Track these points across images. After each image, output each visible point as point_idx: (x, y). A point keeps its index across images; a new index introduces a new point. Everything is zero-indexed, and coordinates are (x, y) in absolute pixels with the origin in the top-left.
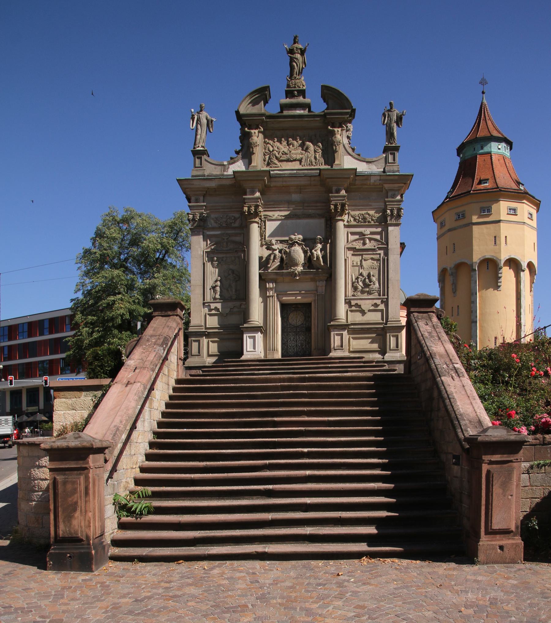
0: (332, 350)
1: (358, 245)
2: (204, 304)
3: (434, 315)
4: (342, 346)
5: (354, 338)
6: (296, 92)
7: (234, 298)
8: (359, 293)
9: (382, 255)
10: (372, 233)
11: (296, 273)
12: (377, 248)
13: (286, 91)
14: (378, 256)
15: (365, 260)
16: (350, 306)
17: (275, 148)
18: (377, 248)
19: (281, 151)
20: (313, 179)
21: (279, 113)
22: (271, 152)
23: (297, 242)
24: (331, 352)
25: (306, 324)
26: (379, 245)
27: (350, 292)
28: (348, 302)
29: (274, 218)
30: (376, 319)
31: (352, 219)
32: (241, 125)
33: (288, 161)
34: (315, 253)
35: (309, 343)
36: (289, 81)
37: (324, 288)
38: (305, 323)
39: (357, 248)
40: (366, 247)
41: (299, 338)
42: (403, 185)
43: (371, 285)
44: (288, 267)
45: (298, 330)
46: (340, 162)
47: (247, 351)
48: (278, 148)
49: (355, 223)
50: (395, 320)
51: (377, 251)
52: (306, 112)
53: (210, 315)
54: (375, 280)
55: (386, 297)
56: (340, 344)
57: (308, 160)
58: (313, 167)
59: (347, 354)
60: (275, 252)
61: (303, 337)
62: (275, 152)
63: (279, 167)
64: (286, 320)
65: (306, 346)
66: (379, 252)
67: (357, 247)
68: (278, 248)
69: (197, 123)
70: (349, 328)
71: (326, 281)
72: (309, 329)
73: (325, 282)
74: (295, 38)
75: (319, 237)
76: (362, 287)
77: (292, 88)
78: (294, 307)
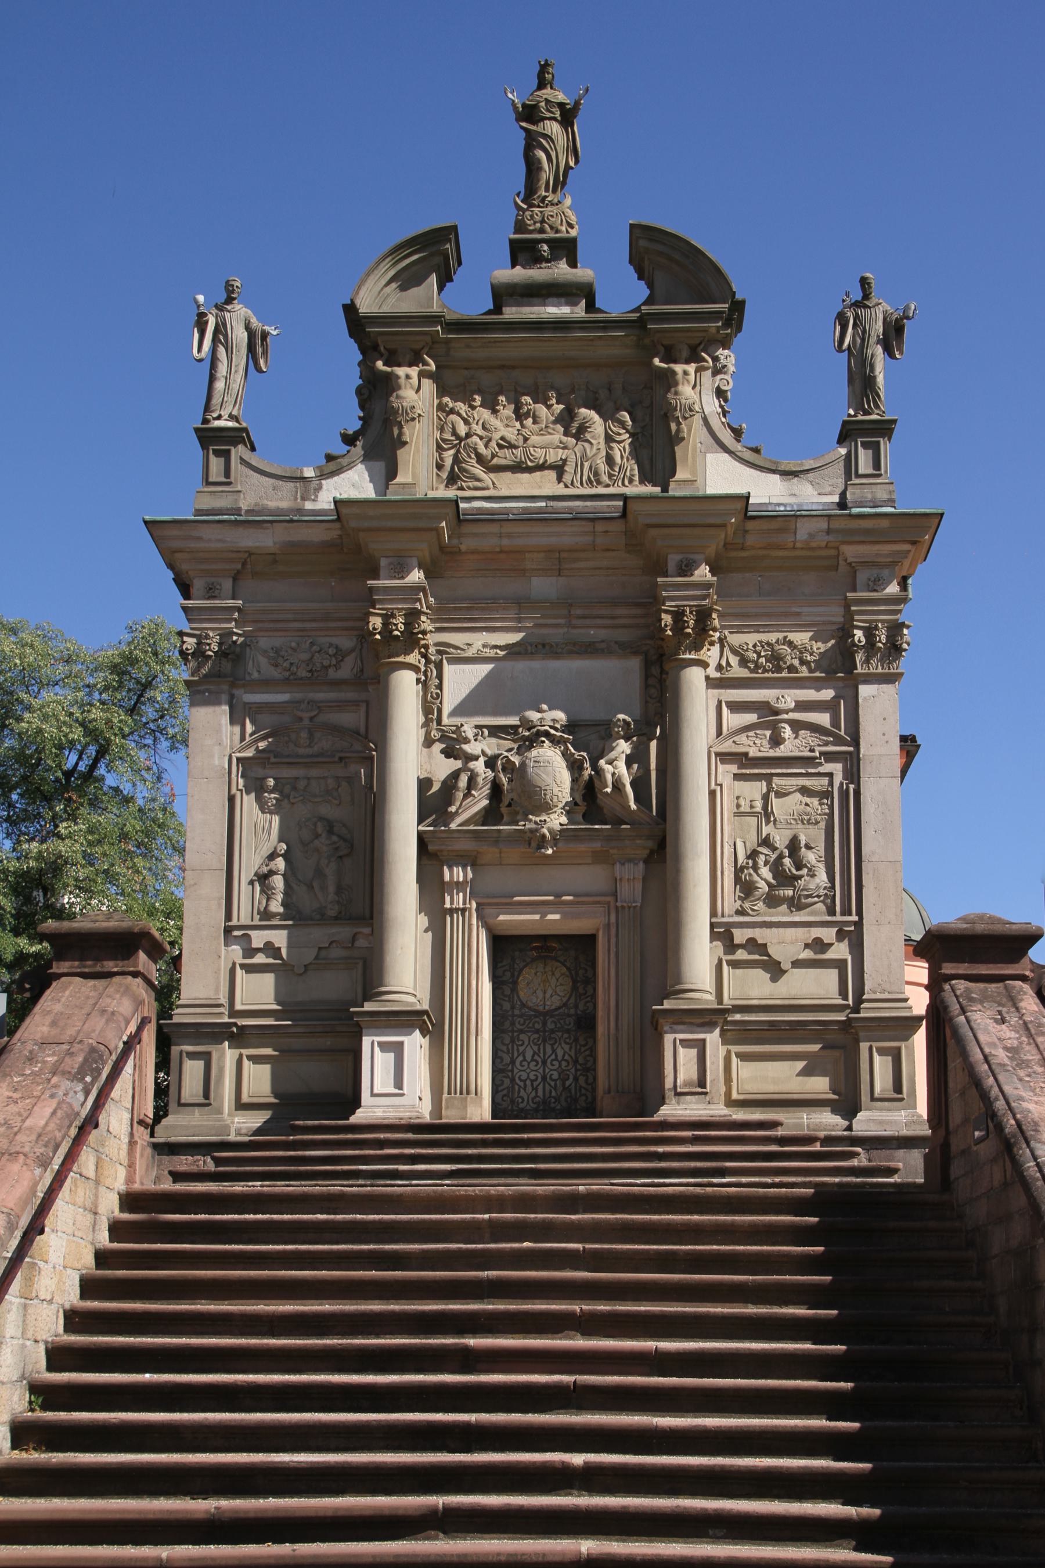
0: (669, 1094)
1: (757, 746)
2: (228, 931)
3: (1026, 987)
4: (702, 1083)
5: (743, 1057)
6: (546, 247)
7: (332, 913)
8: (760, 906)
9: (838, 779)
10: (802, 706)
11: (544, 836)
12: (821, 753)
13: (512, 242)
14: (825, 781)
15: (780, 795)
16: (731, 947)
17: (474, 426)
18: (821, 753)
19: (496, 436)
20: (600, 527)
21: (489, 312)
22: (460, 439)
23: (547, 734)
24: (663, 1104)
25: (576, 1006)
26: (826, 744)
27: (730, 900)
28: (721, 933)
29: (470, 653)
30: (822, 993)
31: (734, 660)
32: (363, 351)
33: (518, 468)
34: (608, 768)
35: (589, 1069)
36: (524, 211)
37: (639, 886)
38: (572, 1000)
39: (751, 754)
40: (782, 751)
41: (554, 1051)
42: (906, 547)
43: (800, 877)
44: (517, 813)
45: (550, 1026)
46: (694, 472)
47: (373, 1095)
48: (484, 428)
49: (744, 673)
50: (886, 996)
51: (821, 764)
52: (578, 311)
53: (249, 969)
54: (814, 862)
55: (854, 918)
56: (694, 1075)
57: (586, 465)
58: (601, 490)
59: (719, 1110)
60: (472, 765)
61: (567, 1047)
62: (475, 439)
63: (487, 488)
64: (508, 992)
65: (576, 1079)
66: (827, 767)
67: (753, 752)
68: (484, 753)
69: (215, 340)
70: (726, 1022)
71: (647, 861)
72: (587, 1023)
73: (641, 865)
74: (544, 68)
75: (621, 716)
76: (769, 884)
77: (531, 232)
78: (535, 948)
